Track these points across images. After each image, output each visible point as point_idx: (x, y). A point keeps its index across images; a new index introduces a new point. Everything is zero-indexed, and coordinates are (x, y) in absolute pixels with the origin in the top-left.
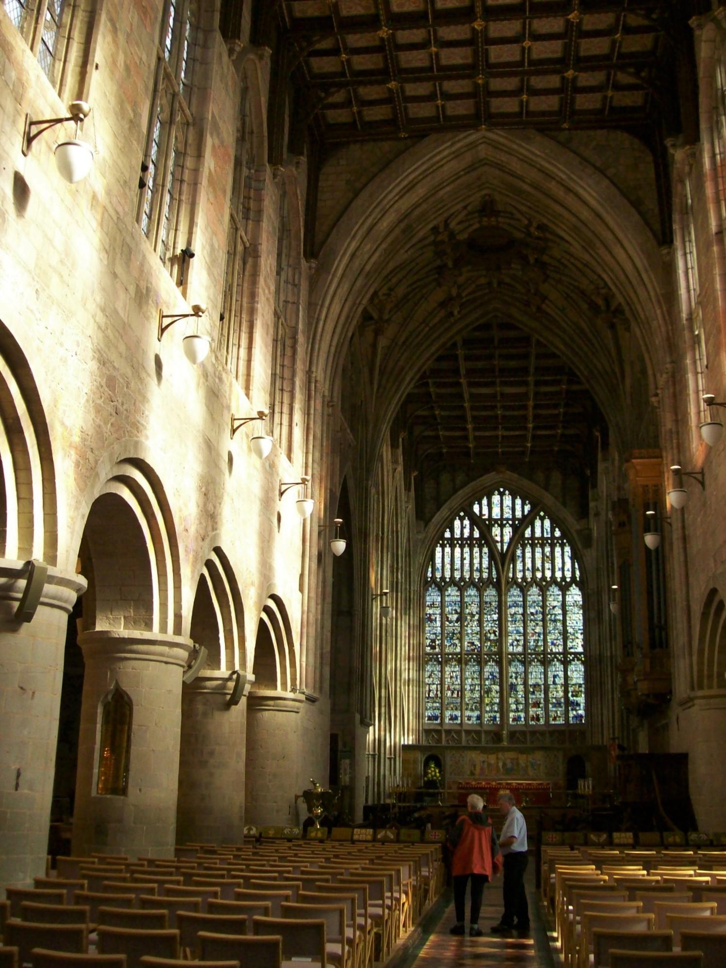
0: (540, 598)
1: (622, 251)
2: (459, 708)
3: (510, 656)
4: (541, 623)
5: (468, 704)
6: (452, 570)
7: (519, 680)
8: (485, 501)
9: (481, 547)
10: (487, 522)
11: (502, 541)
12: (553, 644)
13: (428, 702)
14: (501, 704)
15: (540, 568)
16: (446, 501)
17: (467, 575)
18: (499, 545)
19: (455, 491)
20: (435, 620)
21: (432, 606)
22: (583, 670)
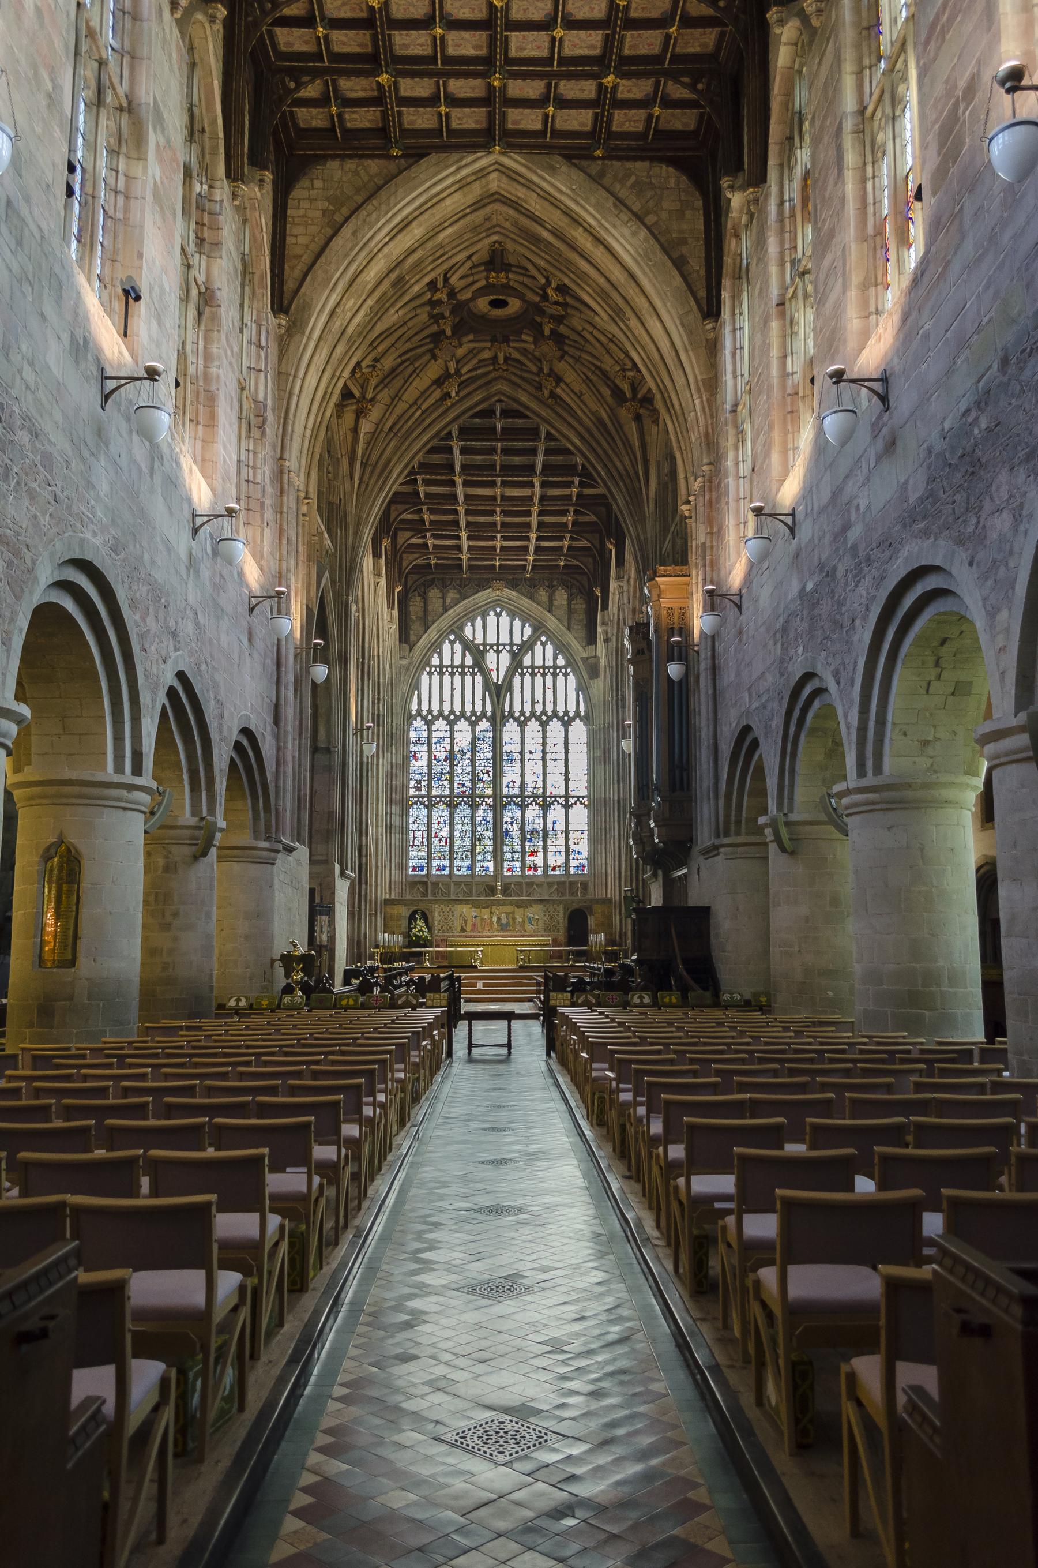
1: (658, 324)
6: (441, 701)
7: (515, 826)
8: (479, 622)
9: (473, 674)
10: (481, 648)
11: (498, 670)
14: (495, 851)
15: (541, 701)
16: (434, 622)
17: (457, 708)
18: (494, 674)
19: (446, 610)
21: (418, 742)
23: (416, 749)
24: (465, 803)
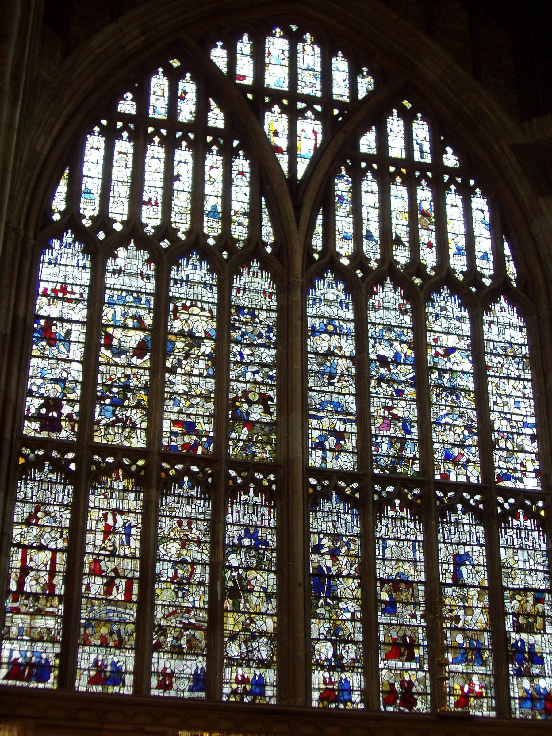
0: (407, 319)
2: (131, 642)
3: (313, 481)
4: (410, 392)
5: (163, 630)
7: (343, 560)
11: (292, 150)
12: (448, 457)
13: (17, 611)
15: (405, 239)
20: (67, 339)
22: (544, 547)
23: (54, 311)
24: (195, 480)
